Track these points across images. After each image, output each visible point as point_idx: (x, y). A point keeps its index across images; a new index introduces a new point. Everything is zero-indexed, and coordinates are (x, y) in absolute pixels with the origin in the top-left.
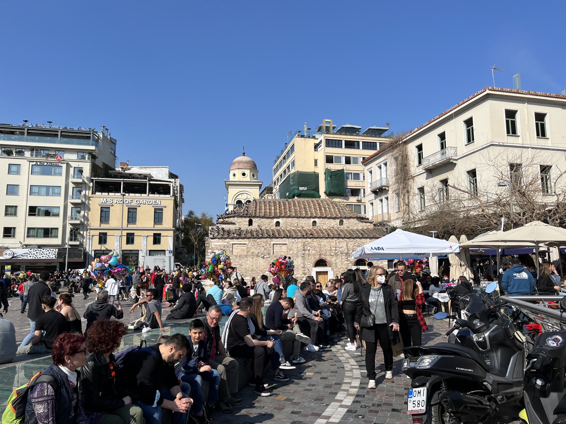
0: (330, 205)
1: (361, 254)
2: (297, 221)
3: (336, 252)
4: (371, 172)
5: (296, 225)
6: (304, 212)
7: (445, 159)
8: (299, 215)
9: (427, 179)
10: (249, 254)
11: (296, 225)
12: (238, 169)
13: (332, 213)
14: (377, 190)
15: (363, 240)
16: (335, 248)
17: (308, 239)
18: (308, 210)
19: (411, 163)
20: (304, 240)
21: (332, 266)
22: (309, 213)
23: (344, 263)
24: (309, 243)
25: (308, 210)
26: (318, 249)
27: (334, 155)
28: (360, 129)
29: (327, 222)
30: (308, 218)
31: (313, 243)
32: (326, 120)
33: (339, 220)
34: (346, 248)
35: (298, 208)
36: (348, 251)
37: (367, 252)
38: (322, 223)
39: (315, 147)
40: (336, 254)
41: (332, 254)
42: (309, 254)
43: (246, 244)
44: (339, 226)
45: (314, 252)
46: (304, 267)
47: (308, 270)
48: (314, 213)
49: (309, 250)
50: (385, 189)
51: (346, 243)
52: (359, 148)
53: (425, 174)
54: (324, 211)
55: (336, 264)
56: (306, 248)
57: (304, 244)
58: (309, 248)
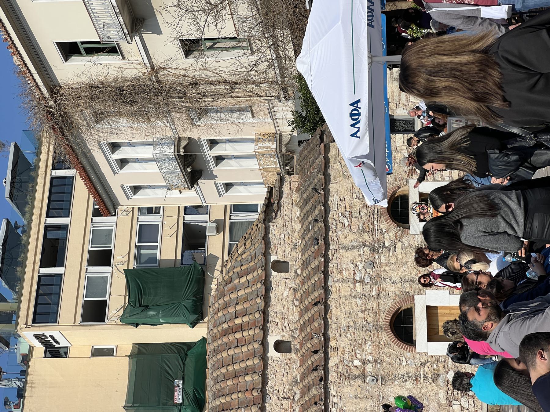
0: (226, 299)
1: (374, 170)
2: (275, 398)
3: (367, 280)
4: (136, 189)
5: (286, 403)
6: (248, 378)
8: (255, 393)
9: (159, 32)
11: (286, 403)
13: (251, 293)
14: (189, 170)
15: (333, 200)
16: (358, 285)
17: (331, 363)
18: (243, 365)
19: (113, 74)
20: (333, 376)
21: (412, 293)
22: (249, 363)
23: (400, 257)
24: (342, 361)
25: (243, 365)
26: (361, 335)
27: (83, 297)
28: (8, 223)
29: (279, 308)
30: (265, 365)
31: (341, 349)
33: (273, 273)
34: (356, 252)
35: (234, 396)
36: (365, 245)
37: (364, 148)
38: (283, 324)
39: (53, 357)
40: (376, 280)
41: (374, 293)
42: (376, 362)
44: (291, 274)
45: (369, 346)
46: (416, 379)
47: (423, 365)
48: (250, 347)
49: (364, 362)
50: (184, 148)
51: (343, 252)
52: (65, 228)
53: (148, 37)
54: (246, 319)
55: (403, 281)
56: (356, 372)
57: (346, 378)
58: (357, 363)
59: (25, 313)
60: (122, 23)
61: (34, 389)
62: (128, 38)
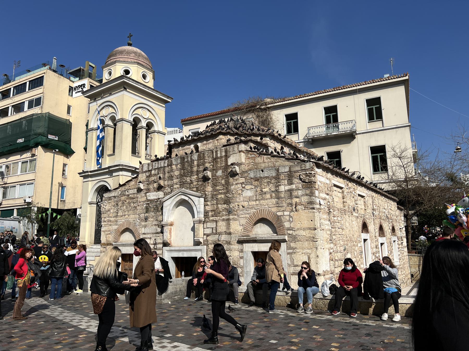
7: (348, 131)
10: (346, 208)
12: (138, 64)
32: (91, 64)
43: (341, 188)
59: (94, 83)
60: (321, 136)
61: (57, 77)
62: (311, 137)
